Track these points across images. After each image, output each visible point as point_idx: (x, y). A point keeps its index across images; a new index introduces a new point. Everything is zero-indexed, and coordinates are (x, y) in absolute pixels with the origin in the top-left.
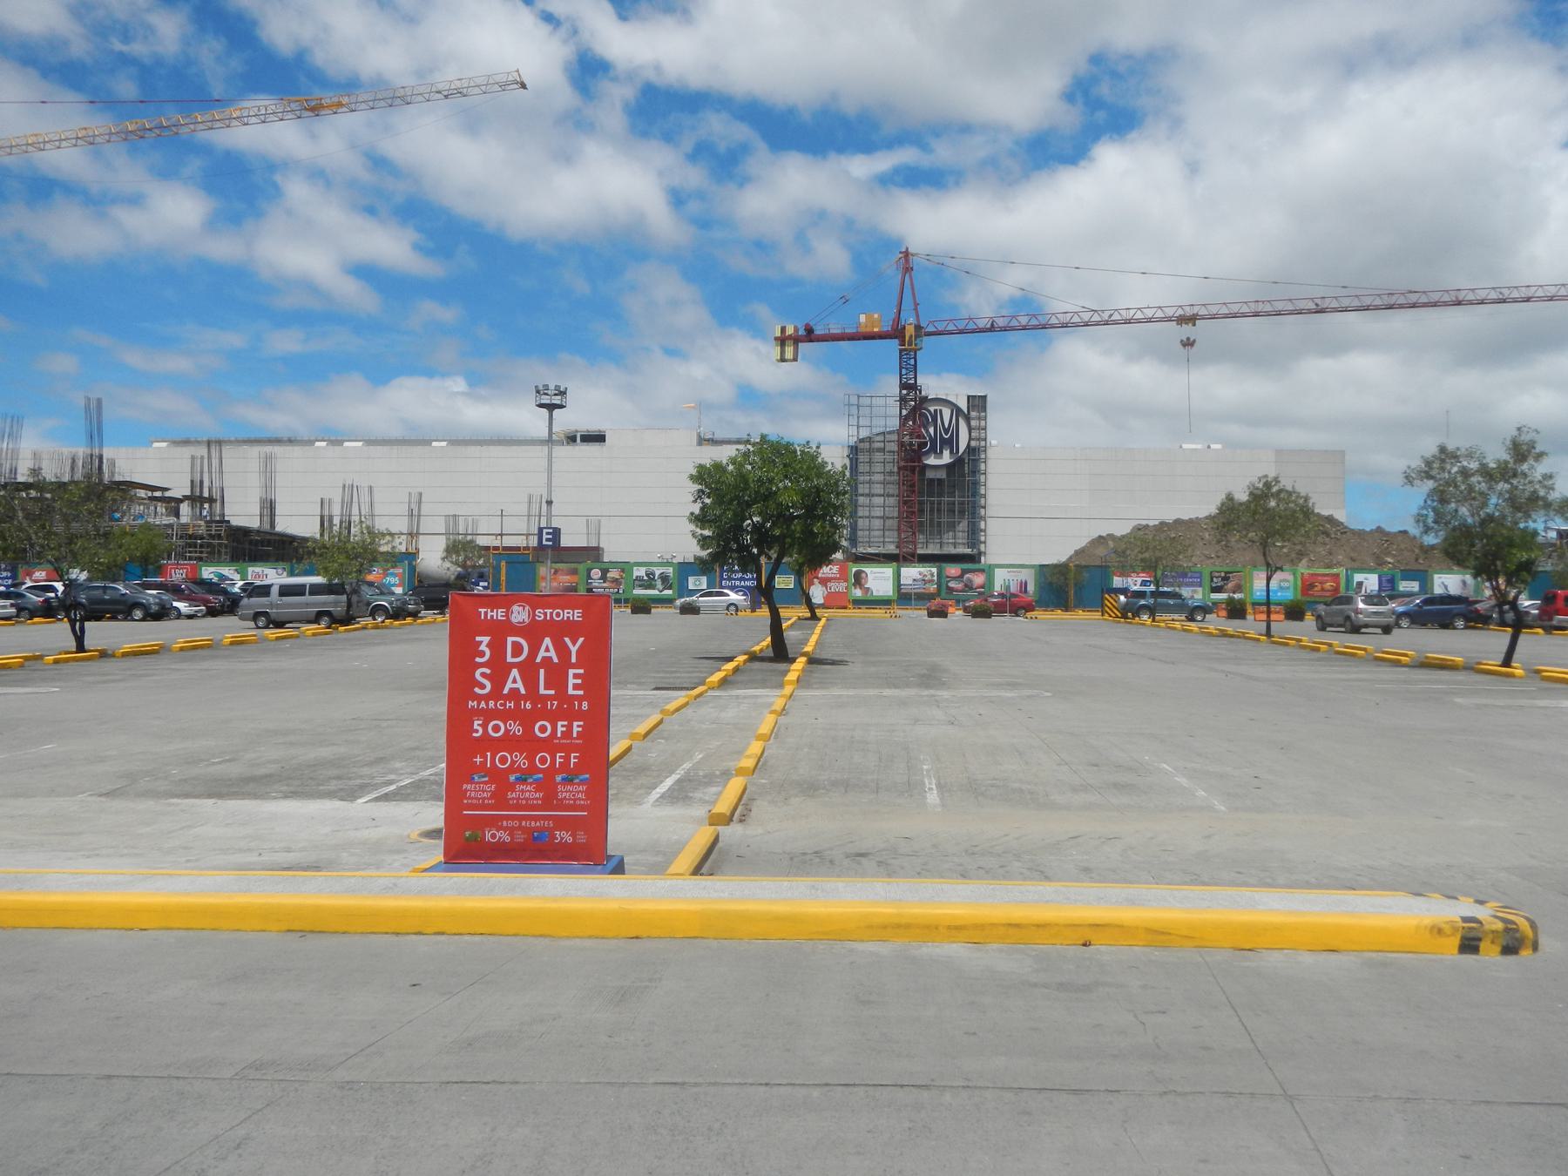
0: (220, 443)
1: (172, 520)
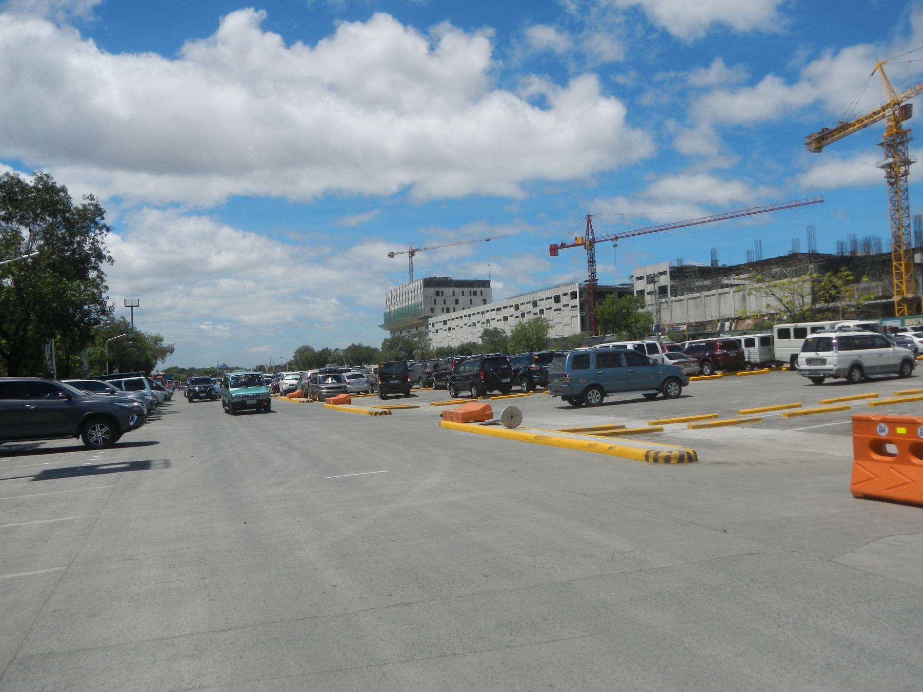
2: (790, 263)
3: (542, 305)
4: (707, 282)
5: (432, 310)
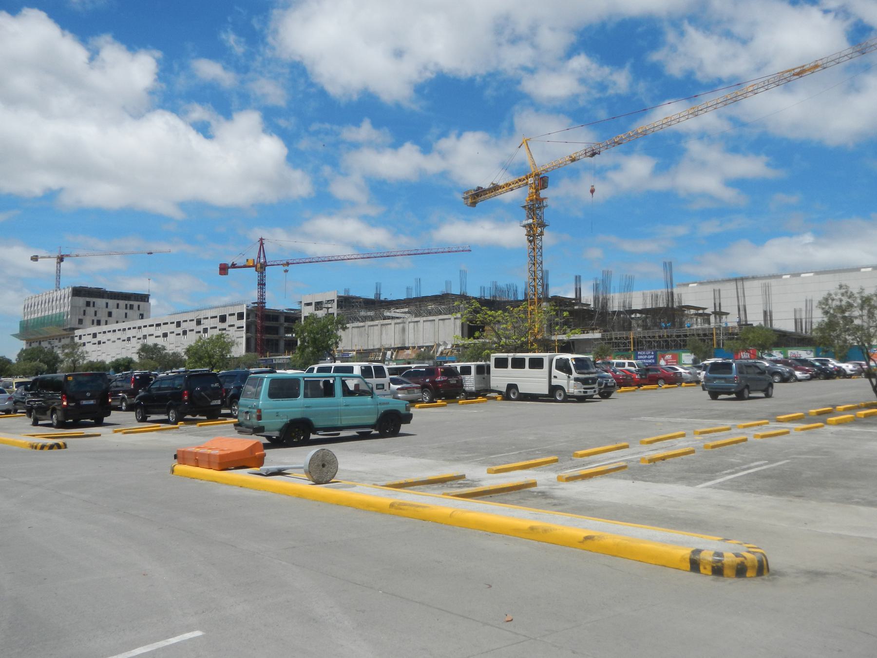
0: (742, 279)
1: (706, 326)
2: (443, 302)
3: (206, 324)
4: (371, 313)
5: (81, 321)
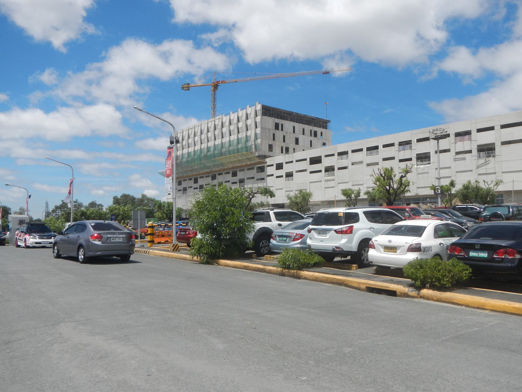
5: (271, 147)
